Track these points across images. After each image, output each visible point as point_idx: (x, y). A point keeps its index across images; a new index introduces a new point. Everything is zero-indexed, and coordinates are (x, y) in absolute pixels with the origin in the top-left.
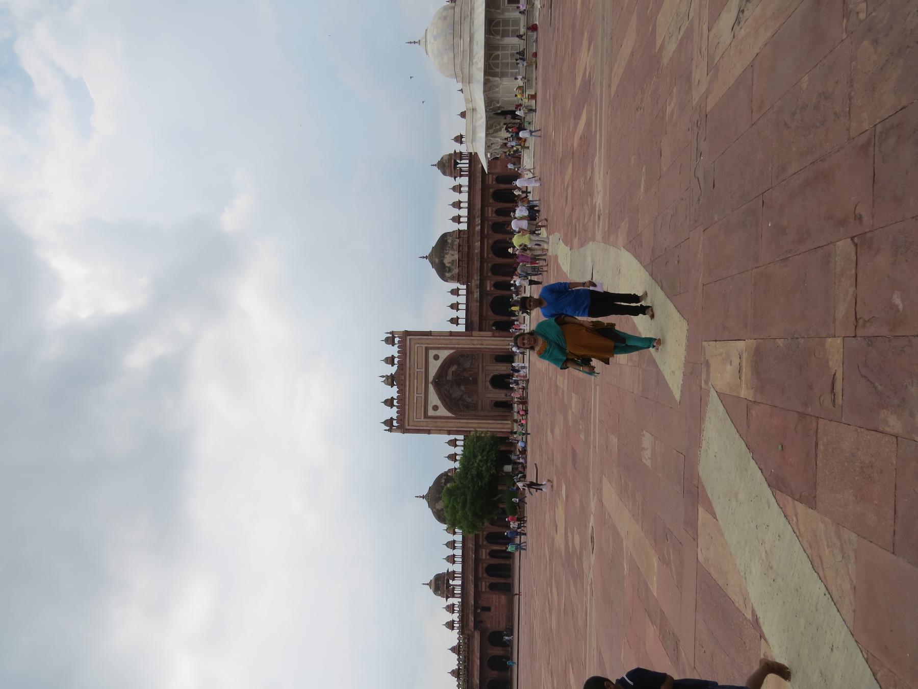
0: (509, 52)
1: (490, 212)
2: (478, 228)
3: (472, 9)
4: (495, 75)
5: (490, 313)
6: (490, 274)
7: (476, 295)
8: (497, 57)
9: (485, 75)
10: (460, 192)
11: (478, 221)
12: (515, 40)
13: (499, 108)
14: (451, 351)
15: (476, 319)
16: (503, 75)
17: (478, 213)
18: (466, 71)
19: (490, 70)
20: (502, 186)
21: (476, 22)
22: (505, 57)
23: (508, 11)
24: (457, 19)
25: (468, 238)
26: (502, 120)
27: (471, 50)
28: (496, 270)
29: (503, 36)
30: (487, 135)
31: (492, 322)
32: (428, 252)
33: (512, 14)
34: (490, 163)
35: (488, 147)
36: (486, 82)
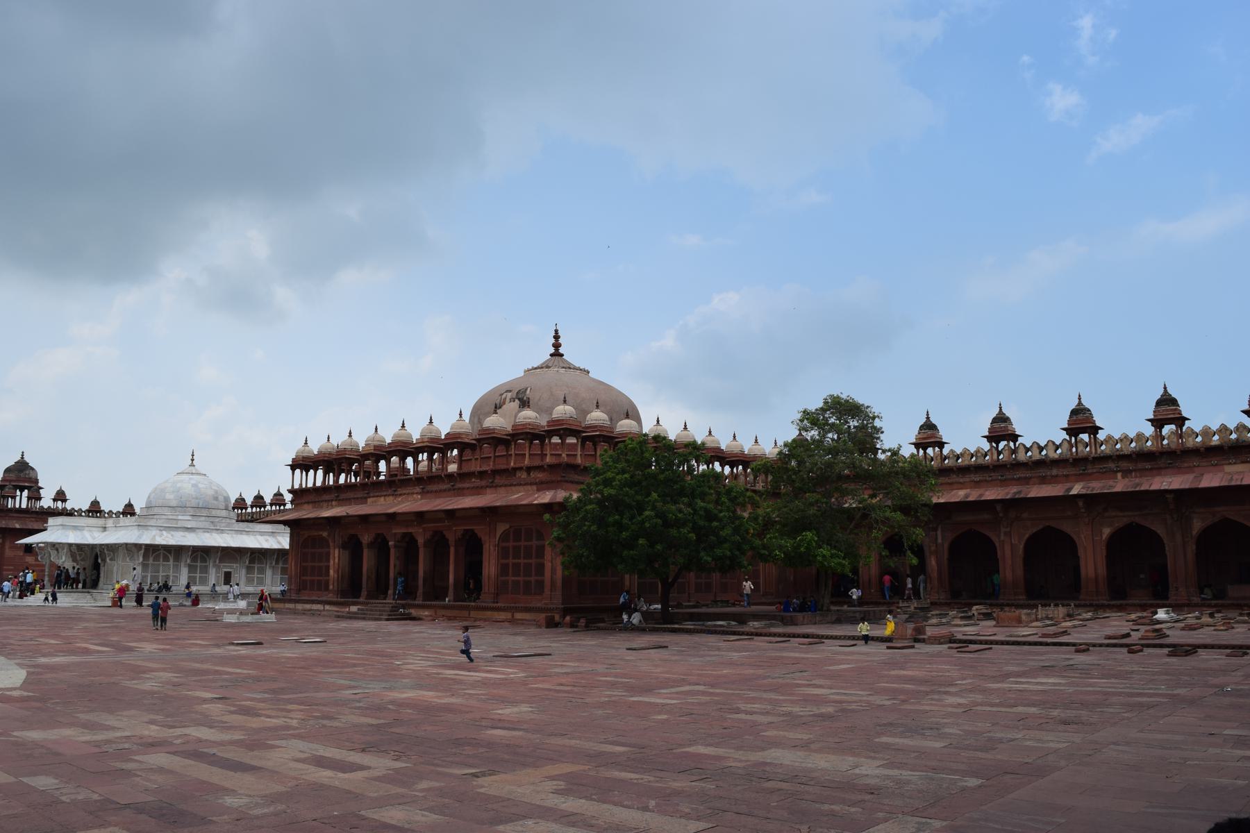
0: (171, 573)
3: (222, 531)
4: (146, 556)
8: (166, 559)
9: (147, 545)
12: (184, 580)
13: (104, 560)
16: (145, 566)
18: (152, 522)
19: (152, 551)
21: (207, 535)
22: (165, 570)
23: (217, 572)
24: (214, 513)
26: (88, 563)
27: (177, 529)
29: (190, 566)
30: (70, 545)
33: (213, 576)
34: (29, 548)
35: (55, 546)
36: (138, 546)
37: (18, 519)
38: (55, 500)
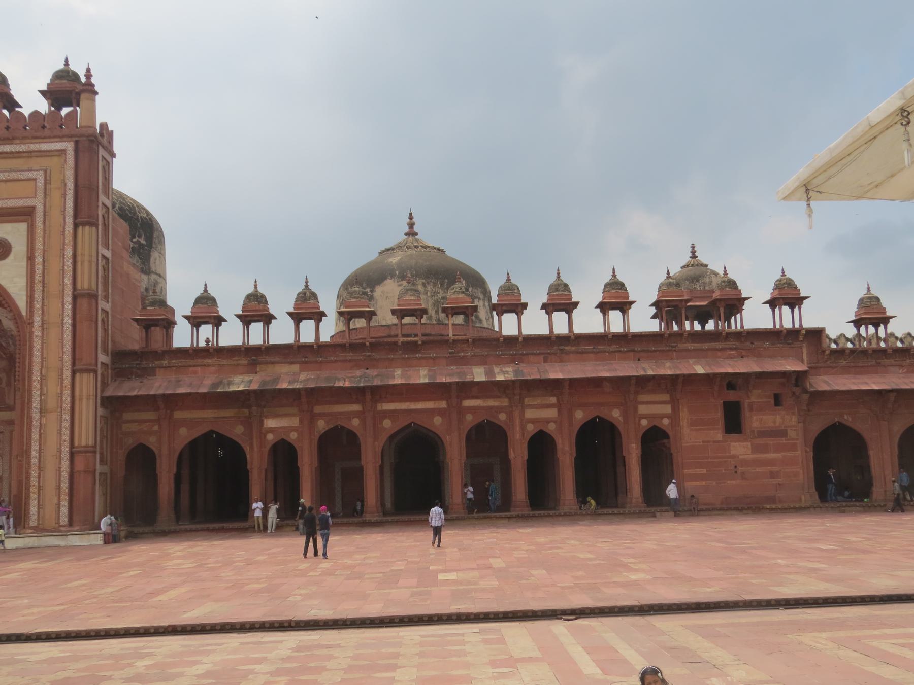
1: (541, 413)
2: (479, 374)
5: (185, 435)
6: (322, 425)
7: (239, 383)
10: (604, 307)
11: (504, 373)
14: (22, 303)
15: (158, 385)
17: (531, 372)
20: (633, 452)
25: (442, 342)
28: (338, 445)
31: (151, 441)
32: (426, 236)
37: (699, 354)
38: (773, 303)
